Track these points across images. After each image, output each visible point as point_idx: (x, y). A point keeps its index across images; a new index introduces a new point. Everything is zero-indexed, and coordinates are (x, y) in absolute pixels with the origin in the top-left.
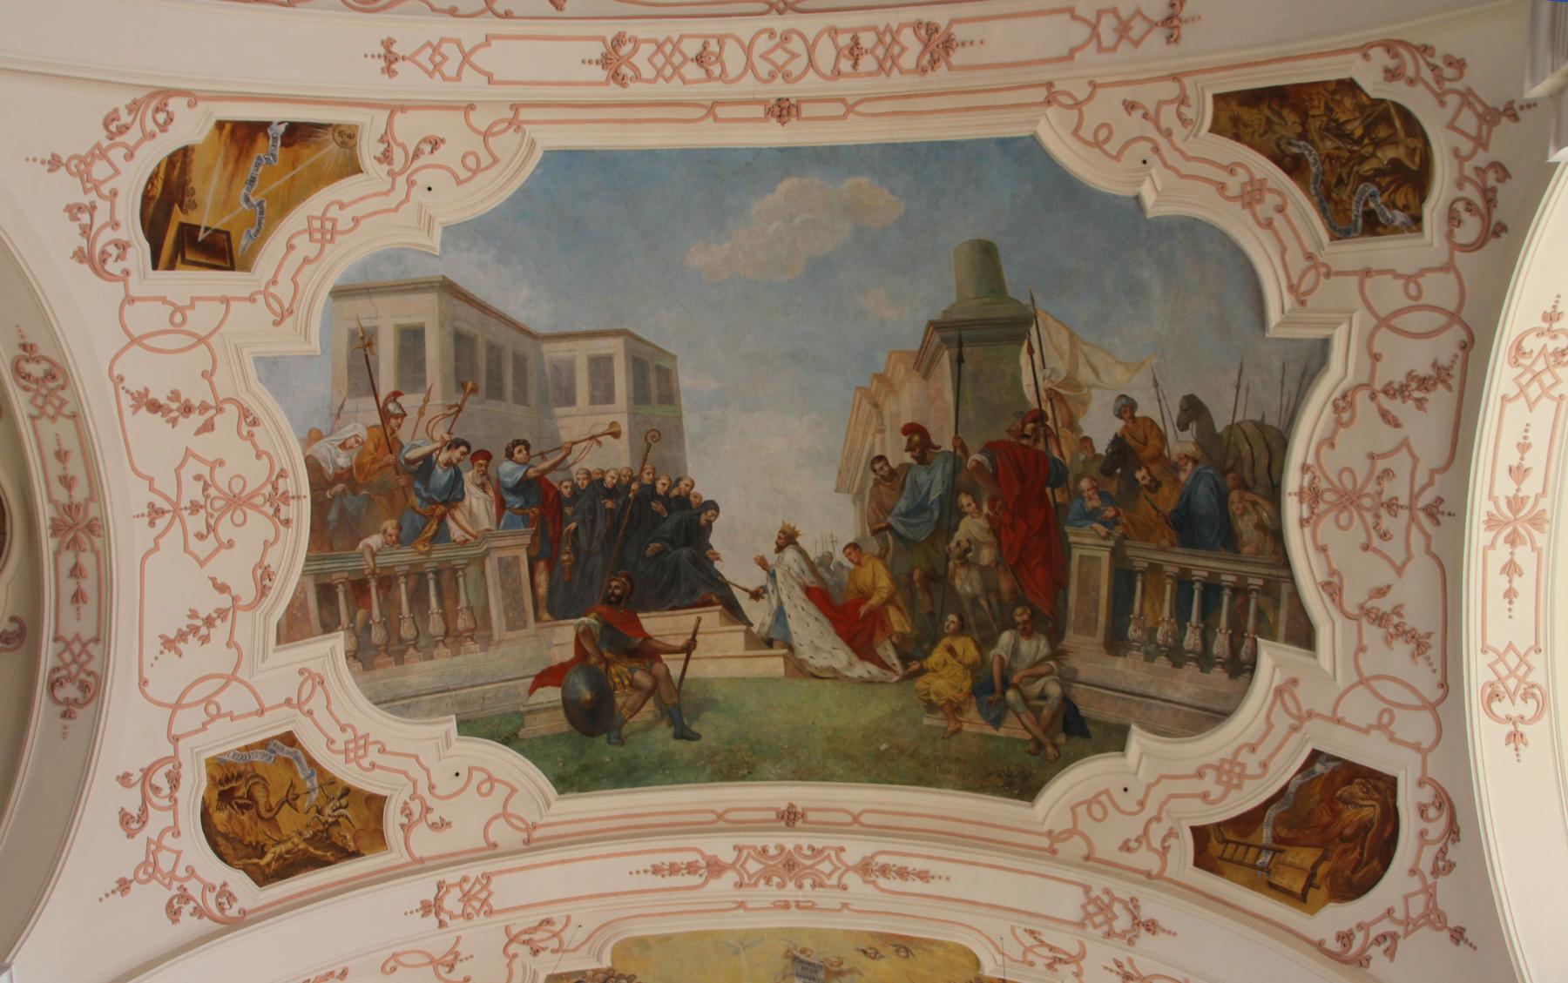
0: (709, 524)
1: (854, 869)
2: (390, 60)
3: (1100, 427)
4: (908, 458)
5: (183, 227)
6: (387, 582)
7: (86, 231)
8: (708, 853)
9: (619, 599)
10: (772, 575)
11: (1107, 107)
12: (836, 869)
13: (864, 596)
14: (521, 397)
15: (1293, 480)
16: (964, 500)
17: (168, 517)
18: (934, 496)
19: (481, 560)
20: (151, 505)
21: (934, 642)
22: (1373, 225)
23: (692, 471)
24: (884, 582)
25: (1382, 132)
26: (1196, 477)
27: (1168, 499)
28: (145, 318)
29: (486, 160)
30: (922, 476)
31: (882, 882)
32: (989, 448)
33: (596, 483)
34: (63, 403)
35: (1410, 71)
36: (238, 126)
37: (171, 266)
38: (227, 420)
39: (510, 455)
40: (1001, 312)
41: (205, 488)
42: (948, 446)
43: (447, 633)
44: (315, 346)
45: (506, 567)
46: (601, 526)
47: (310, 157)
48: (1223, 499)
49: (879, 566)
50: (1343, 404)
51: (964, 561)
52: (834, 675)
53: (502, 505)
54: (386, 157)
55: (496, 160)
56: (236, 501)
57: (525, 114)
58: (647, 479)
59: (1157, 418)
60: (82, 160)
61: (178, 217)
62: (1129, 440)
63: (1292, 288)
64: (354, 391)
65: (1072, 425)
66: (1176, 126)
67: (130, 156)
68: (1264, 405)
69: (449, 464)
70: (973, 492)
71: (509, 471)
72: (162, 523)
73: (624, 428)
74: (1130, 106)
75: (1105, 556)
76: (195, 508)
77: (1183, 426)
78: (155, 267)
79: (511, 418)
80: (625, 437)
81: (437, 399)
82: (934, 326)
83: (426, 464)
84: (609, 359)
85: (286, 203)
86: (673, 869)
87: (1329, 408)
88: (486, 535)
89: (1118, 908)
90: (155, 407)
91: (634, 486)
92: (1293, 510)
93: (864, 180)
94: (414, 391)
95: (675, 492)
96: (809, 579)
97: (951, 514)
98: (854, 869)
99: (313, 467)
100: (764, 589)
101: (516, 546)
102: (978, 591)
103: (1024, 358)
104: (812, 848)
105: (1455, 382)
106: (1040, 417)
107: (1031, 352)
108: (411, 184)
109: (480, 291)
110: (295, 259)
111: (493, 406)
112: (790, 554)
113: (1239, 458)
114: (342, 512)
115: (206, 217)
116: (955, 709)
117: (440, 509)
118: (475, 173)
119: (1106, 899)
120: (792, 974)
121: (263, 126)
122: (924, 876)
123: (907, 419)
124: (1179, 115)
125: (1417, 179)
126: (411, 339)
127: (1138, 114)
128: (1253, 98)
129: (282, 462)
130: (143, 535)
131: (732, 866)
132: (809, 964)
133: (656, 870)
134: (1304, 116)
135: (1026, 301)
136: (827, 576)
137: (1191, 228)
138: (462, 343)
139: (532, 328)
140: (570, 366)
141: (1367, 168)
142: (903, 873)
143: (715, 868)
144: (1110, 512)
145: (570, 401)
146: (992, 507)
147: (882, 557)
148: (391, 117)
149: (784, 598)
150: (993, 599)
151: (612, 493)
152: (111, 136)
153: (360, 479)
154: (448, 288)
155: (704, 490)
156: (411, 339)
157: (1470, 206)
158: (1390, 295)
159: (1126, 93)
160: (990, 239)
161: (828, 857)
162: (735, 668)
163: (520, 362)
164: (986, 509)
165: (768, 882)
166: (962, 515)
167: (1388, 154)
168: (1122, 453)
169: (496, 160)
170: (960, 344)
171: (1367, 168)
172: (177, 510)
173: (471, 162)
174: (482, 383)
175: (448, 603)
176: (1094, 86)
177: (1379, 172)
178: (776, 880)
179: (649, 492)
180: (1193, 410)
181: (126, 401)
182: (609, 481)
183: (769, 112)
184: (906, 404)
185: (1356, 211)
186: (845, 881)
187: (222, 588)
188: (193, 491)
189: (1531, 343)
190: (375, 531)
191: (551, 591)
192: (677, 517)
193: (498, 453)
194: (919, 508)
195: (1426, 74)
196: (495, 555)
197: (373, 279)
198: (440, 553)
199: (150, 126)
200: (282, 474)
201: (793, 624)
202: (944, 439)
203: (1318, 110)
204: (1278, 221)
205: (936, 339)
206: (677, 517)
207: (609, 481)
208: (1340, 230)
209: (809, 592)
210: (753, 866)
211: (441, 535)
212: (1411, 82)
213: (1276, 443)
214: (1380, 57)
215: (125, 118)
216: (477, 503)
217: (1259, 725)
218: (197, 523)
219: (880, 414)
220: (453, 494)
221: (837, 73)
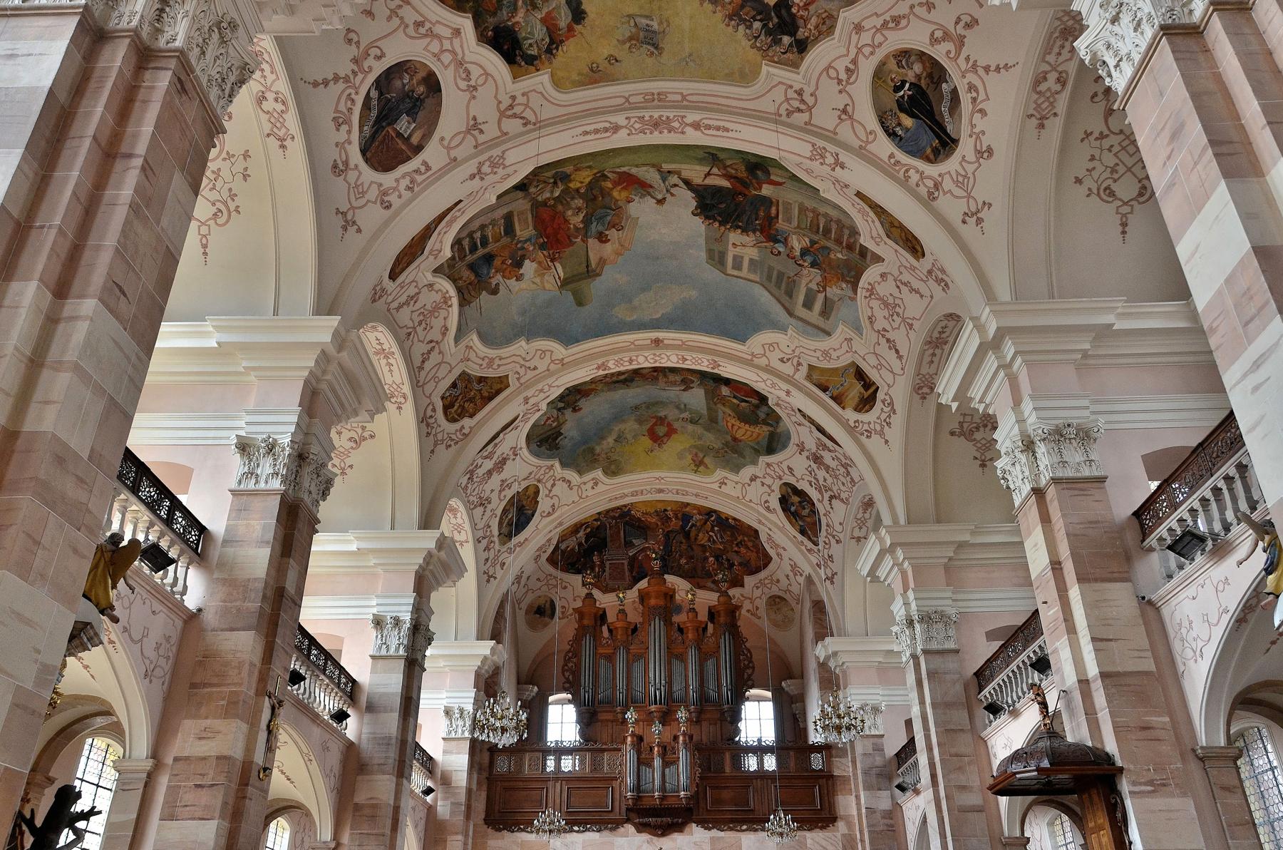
0: (696, 209)
1: (622, 127)
2: (788, 393)
3: (529, 268)
4: (607, 232)
5: (866, 391)
6: (838, 241)
7: (889, 416)
8: (699, 133)
9: (740, 194)
10: (667, 191)
11: (542, 365)
12: (632, 126)
13: (625, 188)
14: (771, 269)
15: (455, 301)
16: (581, 226)
17: (907, 320)
18: (595, 224)
19: (798, 227)
20: (911, 329)
21: (590, 183)
22: (454, 385)
23: (703, 227)
24: (615, 194)
25: (460, 410)
26: (488, 273)
27: (497, 262)
28: (889, 378)
29: (767, 347)
30: (600, 228)
31: (607, 125)
32: (572, 244)
33: (745, 231)
34: (920, 379)
35: (458, 433)
36: (839, 404)
37: (874, 383)
38: (878, 326)
39: (779, 252)
40: (572, 286)
41: (892, 316)
42: (590, 241)
43: (818, 215)
44: (841, 327)
45: (789, 220)
46: (745, 218)
47: (823, 379)
48: (477, 275)
49: (618, 198)
50: (445, 330)
51: (579, 209)
52: (637, 166)
53: (786, 239)
54: (799, 364)
55: (763, 345)
56: (886, 305)
57: (750, 357)
58: (723, 228)
59: (507, 281)
60: (880, 435)
61: (866, 394)
62: (517, 269)
63: (471, 347)
64: (833, 302)
65: (540, 263)
66: (519, 369)
67: (869, 423)
68: (471, 310)
69: (805, 261)
70: (577, 229)
71: (781, 248)
72: (910, 321)
73: (730, 246)
74: (535, 368)
75: (518, 233)
76: (898, 314)
77: (497, 285)
78: (878, 387)
79: (778, 264)
80: (731, 243)
81: (804, 282)
82: (599, 275)
83: (813, 265)
84: (734, 268)
85: (834, 371)
86: (718, 128)
87: (449, 328)
88: (795, 233)
89: (489, 170)
90: (897, 352)
91: (728, 227)
92: (452, 292)
93: (628, 319)
94: (811, 289)
95: (711, 221)
96: (651, 190)
97: (587, 222)
98: (622, 127)
99: (855, 292)
100: (671, 187)
101: (781, 224)
102: (572, 203)
103: (562, 275)
104: (645, 133)
105: (416, 370)
106: (552, 261)
107: (559, 278)
108: (793, 351)
109: (779, 306)
110: (838, 353)
111: (782, 270)
112: (660, 197)
113: (474, 289)
114: (849, 271)
115: (858, 387)
116: (578, 170)
117: (811, 250)
118: (771, 345)
119: (495, 170)
120: (659, 33)
121: (831, 397)
122: (586, 133)
123: (608, 245)
124: (519, 373)
125: (446, 408)
126: (808, 304)
127: (532, 367)
128: (498, 392)
129: (864, 302)
130: (916, 325)
131: (687, 125)
132: (649, 44)
133: (727, 130)
134: (482, 398)
135: (563, 292)
136: (642, 192)
137: (508, 341)
138: (790, 294)
139: (761, 287)
140: (749, 270)
141: (460, 397)
142: (597, 131)
143: (696, 126)
144: (519, 246)
145: (751, 260)
146: (569, 228)
147: (617, 201)
148: (794, 375)
149: (662, 185)
150: (565, 202)
151: (739, 227)
152: (871, 433)
153: (839, 275)
154: (790, 314)
155: (698, 220)
156: (808, 304)
157: (431, 417)
158: (443, 370)
159: (537, 372)
160: (579, 308)
161: (636, 130)
162: (683, 166)
163: (769, 278)
164: (572, 226)
165: (668, 118)
166: (582, 222)
167: (456, 407)
168: (519, 264)
169: (763, 345)
170: (588, 271)
171: (460, 397)
172: (904, 320)
173: (772, 349)
174: (785, 279)
175: (815, 222)
176: (548, 370)
177: (456, 400)
178: (664, 119)
179: (721, 224)
180: (495, 291)
181: (904, 361)
182: (739, 231)
183: (662, 341)
184: (608, 249)
185: (459, 385)
186: (627, 121)
187: (898, 287)
188: (898, 320)
189: (403, 401)
190: (839, 259)
191: (770, 207)
192: (710, 214)
193: (784, 256)
194: (601, 219)
195: (454, 437)
196: (792, 226)
197: (816, 331)
198: (816, 238)
199: (861, 424)
200: (866, 297)
201: (659, 177)
202: (592, 242)
203: (479, 402)
204: (480, 362)
205: (597, 271)
206: (710, 214)
207: (739, 231)
208: (464, 376)
209: (651, 187)
210: (676, 124)
211: (813, 242)
212: (457, 431)
213: (463, 302)
214: (466, 431)
215: (866, 433)
216: (797, 244)
217: (444, 240)
218: (898, 309)
219: (619, 243)
220: (804, 252)
221: (637, 356)
